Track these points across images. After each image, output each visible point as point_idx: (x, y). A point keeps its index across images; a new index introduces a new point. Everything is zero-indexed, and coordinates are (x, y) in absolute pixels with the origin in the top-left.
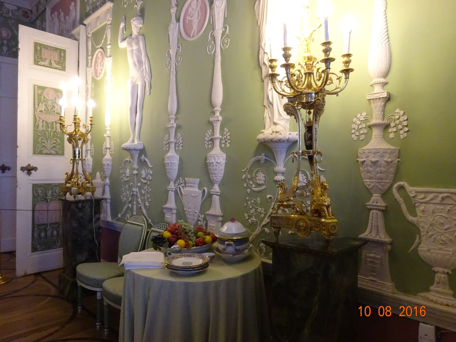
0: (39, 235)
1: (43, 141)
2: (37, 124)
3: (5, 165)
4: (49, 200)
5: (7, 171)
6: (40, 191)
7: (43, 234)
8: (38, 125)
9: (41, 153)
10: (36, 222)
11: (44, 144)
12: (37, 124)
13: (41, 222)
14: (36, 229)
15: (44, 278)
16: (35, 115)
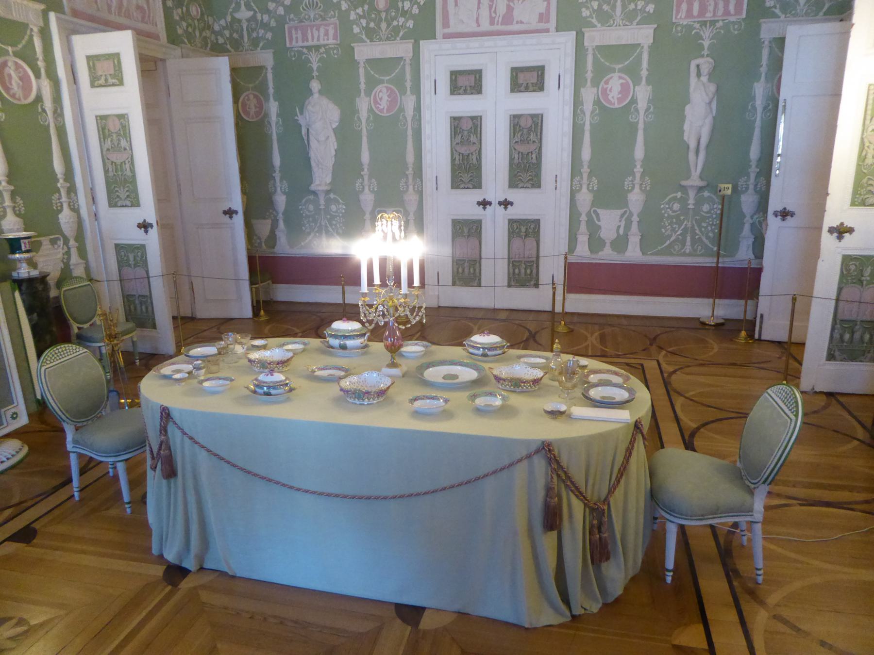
0: (842, 336)
1: (871, 182)
2: (864, 153)
3: (788, 209)
4: (865, 283)
5: (789, 217)
6: (853, 267)
7: (847, 336)
8: (866, 155)
9: (863, 204)
10: (840, 316)
11: (870, 188)
12: (864, 153)
13: (848, 317)
14: (838, 326)
15: (838, 401)
16: (862, 140)
